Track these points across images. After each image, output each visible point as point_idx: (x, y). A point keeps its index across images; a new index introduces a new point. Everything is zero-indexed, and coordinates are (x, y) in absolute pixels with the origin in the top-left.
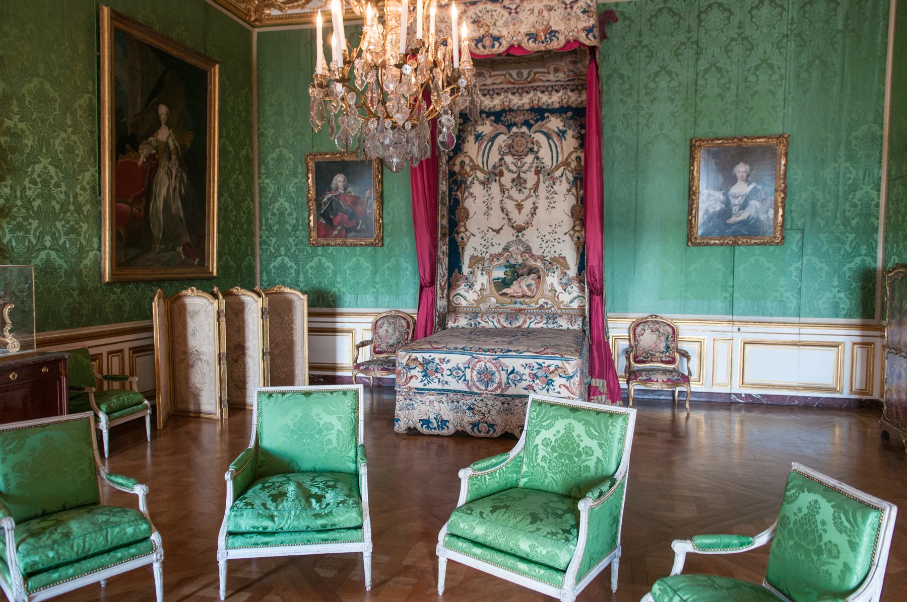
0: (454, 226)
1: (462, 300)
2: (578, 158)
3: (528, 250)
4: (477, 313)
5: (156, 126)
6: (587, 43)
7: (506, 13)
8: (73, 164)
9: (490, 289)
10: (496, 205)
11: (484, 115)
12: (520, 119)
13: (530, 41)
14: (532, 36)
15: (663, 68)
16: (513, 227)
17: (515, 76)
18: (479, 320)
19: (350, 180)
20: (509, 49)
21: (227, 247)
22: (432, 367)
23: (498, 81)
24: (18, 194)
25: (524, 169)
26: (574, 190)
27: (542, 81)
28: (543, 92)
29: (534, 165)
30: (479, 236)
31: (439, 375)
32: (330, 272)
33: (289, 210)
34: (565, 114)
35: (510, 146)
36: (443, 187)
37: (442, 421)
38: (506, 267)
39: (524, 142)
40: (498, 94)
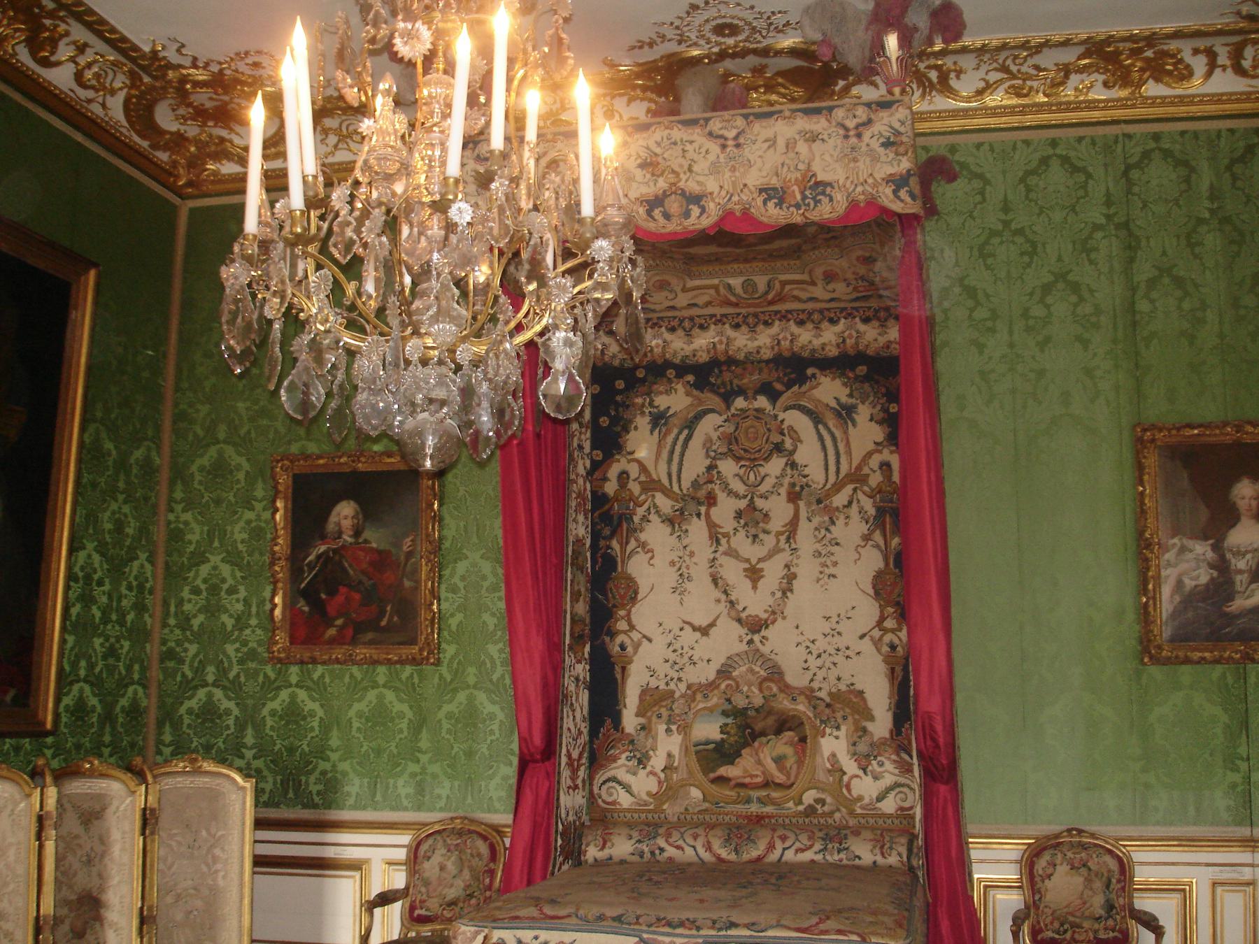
1: (622, 792)
2: (885, 466)
3: (775, 674)
4: (657, 825)
6: (897, 207)
7: (714, 148)
10: (700, 571)
11: (671, 373)
12: (752, 379)
13: (771, 204)
16: (739, 621)
17: (739, 290)
18: (661, 842)
19: (369, 513)
25: (763, 488)
26: (878, 536)
29: (787, 481)
30: (660, 641)
33: (230, 581)
34: (853, 369)
35: (731, 439)
36: (579, 528)
38: (725, 714)
39: (762, 430)
40: (702, 327)
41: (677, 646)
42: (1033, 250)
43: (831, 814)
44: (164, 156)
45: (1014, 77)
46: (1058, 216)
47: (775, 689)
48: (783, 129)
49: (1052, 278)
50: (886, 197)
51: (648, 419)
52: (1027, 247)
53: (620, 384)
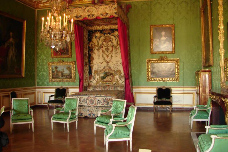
0: (90, 62)
3: (110, 68)
4: (95, 86)
5: (9, 38)
6: (115, 16)
7: (95, 9)
9: (100, 80)
10: (101, 56)
11: (97, 31)
12: (108, 32)
16: (106, 62)
17: (105, 21)
20: (96, 18)
25: (108, 46)
27: (112, 22)
28: (113, 25)
29: (111, 45)
30: (96, 64)
35: (105, 40)
36: (86, 51)
38: (104, 73)
43: (116, 85)
47: (110, 70)
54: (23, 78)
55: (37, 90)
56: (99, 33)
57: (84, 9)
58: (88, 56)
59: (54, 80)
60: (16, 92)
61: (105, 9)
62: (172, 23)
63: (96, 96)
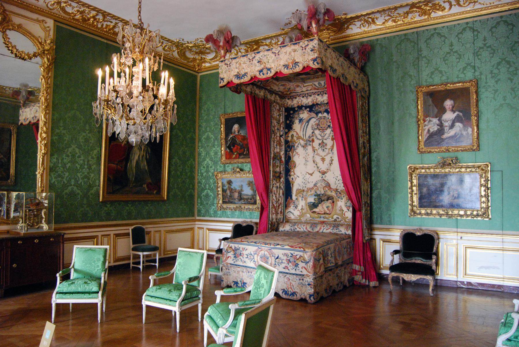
0: (288, 171)
3: (328, 185)
6: (314, 67)
7: (273, 55)
8: (88, 147)
9: (306, 208)
10: (310, 160)
11: (304, 108)
12: (323, 109)
14: (286, 66)
15: (437, 69)
17: (318, 85)
21: (191, 185)
22: (238, 252)
23: (309, 89)
24: (60, 161)
25: (325, 137)
30: (301, 177)
31: (241, 257)
32: (212, 198)
35: (318, 125)
37: (244, 283)
38: (315, 195)
40: (310, 96)
41: (305, 178)
42: (460, 57)
43: (340, 221)
44: (192, 64)
45: (393, 18)
46: (502, 40)
47: (327, 189)
48: (288, 49)
49: (501, 60)
50: (312, 65)
51: (298, 121)
52: (458, 56)
53: (292, 112)
54: (164, 201)
55: (198, 224)
56: (306, 112)
57: (251, 58)
58: (283, 159)
59: (225, 206)
60: (144, 227)
61: (293, 53)
62: (472, 78)
63: (274, 248)
